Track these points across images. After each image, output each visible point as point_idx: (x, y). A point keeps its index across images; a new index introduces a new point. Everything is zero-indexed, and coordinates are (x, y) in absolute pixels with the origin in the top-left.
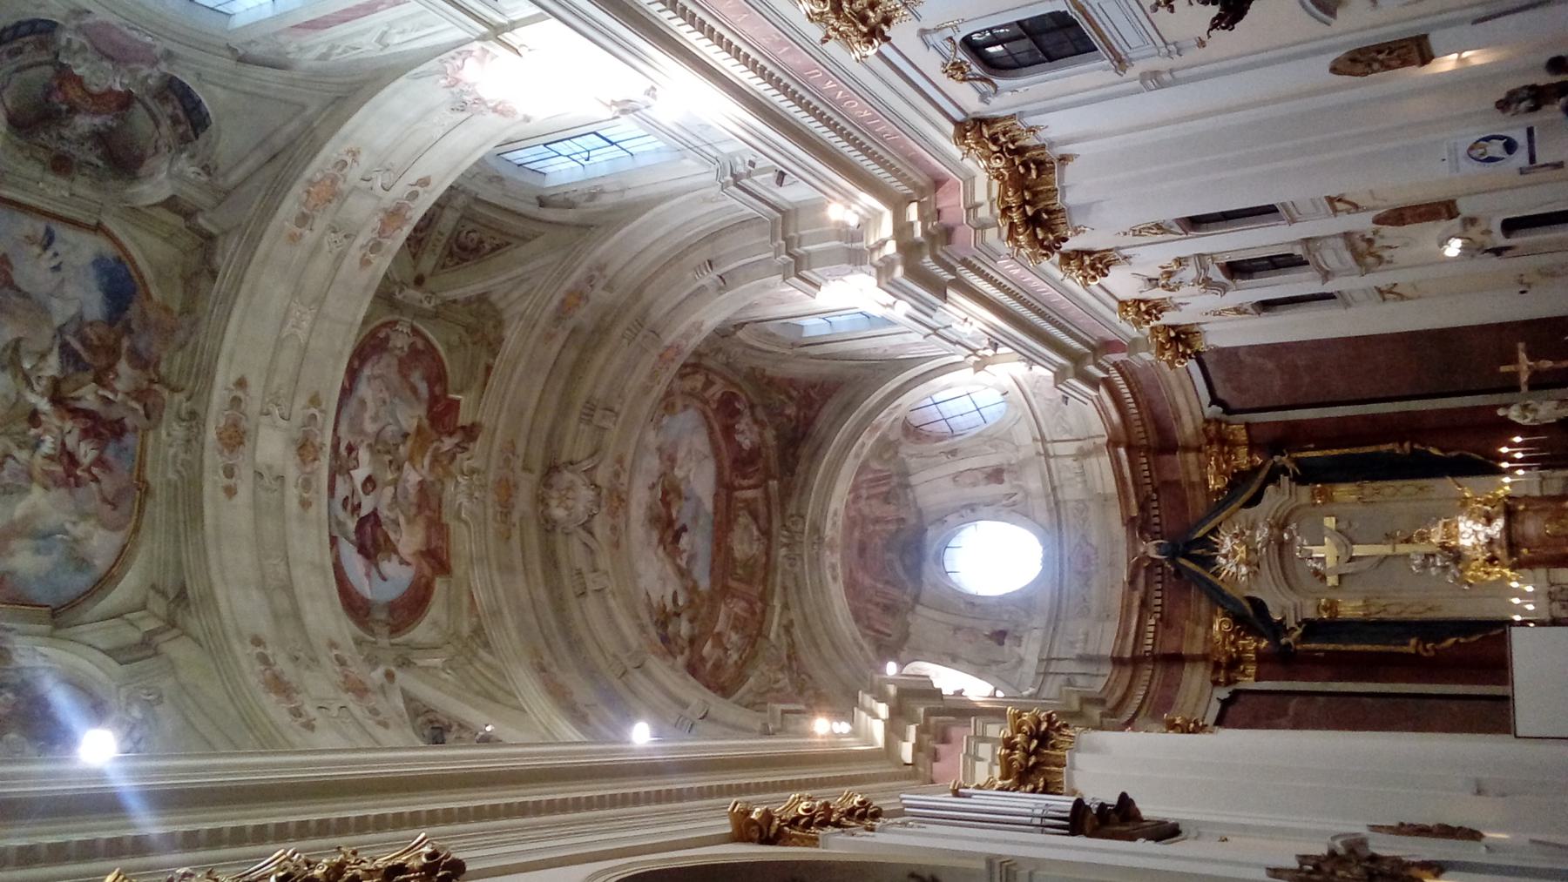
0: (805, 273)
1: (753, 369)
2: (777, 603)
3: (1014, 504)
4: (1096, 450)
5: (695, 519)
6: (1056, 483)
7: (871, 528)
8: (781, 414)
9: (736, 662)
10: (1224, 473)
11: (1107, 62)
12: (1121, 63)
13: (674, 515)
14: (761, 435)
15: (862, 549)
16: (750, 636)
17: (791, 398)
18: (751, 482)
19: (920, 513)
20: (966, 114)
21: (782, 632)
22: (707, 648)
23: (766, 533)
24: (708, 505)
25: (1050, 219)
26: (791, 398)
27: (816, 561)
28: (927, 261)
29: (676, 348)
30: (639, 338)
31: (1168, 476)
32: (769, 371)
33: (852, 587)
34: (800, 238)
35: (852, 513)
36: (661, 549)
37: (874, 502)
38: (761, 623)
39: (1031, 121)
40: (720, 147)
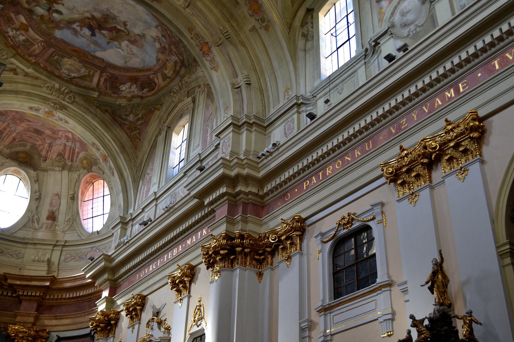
0: (231, 129)
1: (161, 105)
2: (30, 71)
3: (33, 222)
4: (49, 271)
5: (96, 43)
6: (38, 246)
7: (48, 141)
8: (131, 112)
9: (8, 33)
10: (16, 335)
11: (327, 301)
12: (325, 310)
13: (104, 32)
14: (125, 97)
15: (37, 132)
16: (19, 47)
17: (138, 120)
18: (101, 83)
19: (45, 170)
20: (309, 226)
21: (14, 67)
22: (22, 19)
23: (70, 81)
24: (99, 54)
25: (229, 259)
26: (138, 120)
27: (45, 100)
28: (223, 190)
29: (207, 52)
30: (221, 36)
31: (24, 304)
32: (157, 113)
33: (20, 117)
34: (251, 132)
35: (60, 133)
36: (88, 15)
37: (62, 148)
38: (23, 57)
39: (296, 259)
40: (333, 93)
